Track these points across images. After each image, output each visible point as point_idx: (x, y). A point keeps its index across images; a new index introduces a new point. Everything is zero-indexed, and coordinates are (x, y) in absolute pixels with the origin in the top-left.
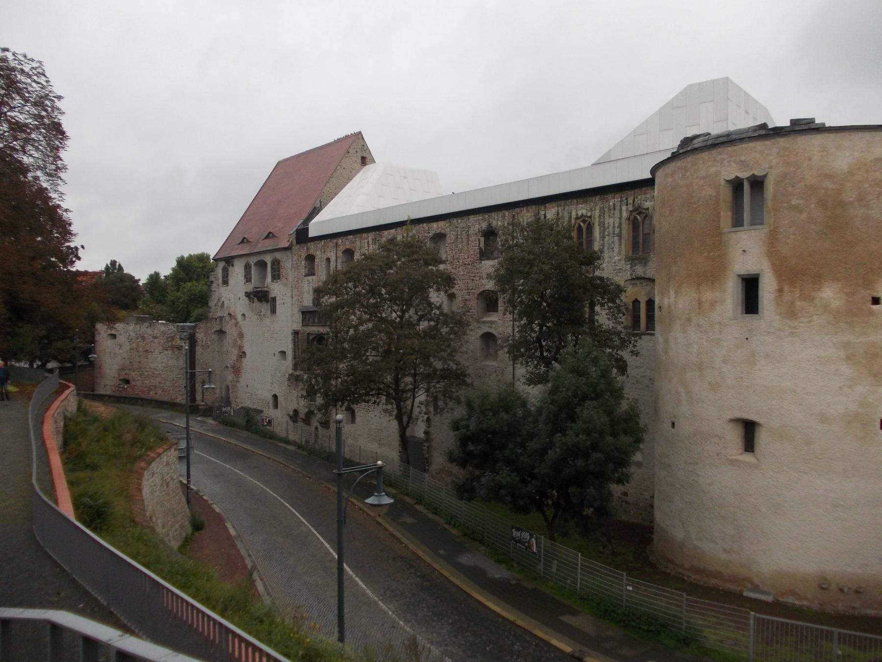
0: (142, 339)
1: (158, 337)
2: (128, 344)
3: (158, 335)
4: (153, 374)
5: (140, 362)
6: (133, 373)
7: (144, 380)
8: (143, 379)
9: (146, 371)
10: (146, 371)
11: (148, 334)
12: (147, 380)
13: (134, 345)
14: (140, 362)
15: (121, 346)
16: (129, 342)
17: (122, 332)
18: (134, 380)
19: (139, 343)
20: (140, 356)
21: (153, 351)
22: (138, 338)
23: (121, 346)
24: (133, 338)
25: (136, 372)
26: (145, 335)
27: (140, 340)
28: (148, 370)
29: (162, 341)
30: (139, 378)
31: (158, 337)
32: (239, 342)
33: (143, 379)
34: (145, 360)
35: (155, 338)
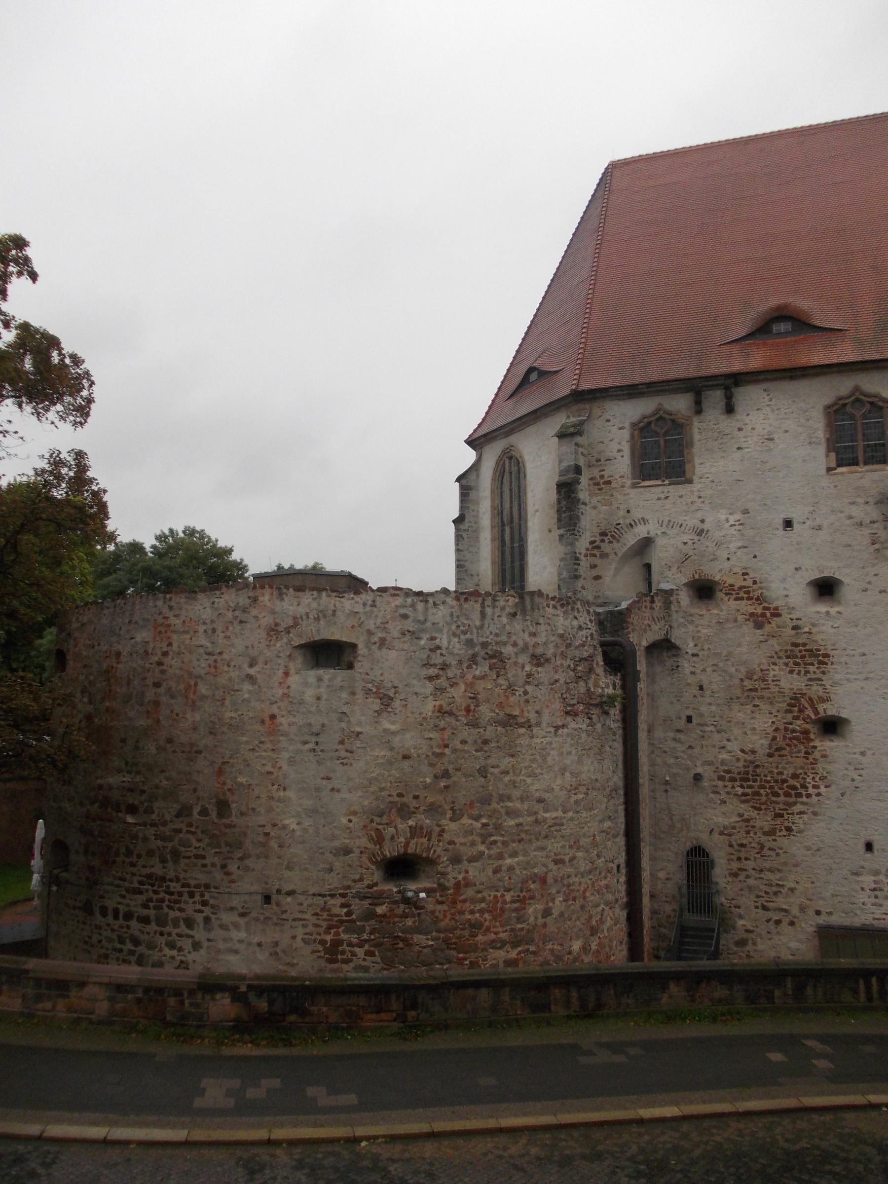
0: (491, 669)
1: (548, 660)
2: (429, 688)
3: (550, 651)
4: (537, 821)
5: (483, 772)
6: (453, 826)
7: (500, 856)
8: (495, 851)
9: (510, 813)
10: (510, 813)
11: (515, 644)
12: (514, 854)
13: (458, 693)
14: (483, 772)
15: (386, 701)
16: (430, 678)
17: (396, 633)
18: (456, 860)
19: (481, 686)
20: (486, 742)
21: (532, 716)
22: (473, 660)
23: (386, 701)
24: (450, 660)
25: (465, 820)
26: (508, 650)
27: (482, 669)
28: (518, 805)
29: (561, 677)
30: (482, 848)
31: (548, 660)
32: (793, 682)
33: (495, 851)
34: (506, 762)
35: (539, 665)
